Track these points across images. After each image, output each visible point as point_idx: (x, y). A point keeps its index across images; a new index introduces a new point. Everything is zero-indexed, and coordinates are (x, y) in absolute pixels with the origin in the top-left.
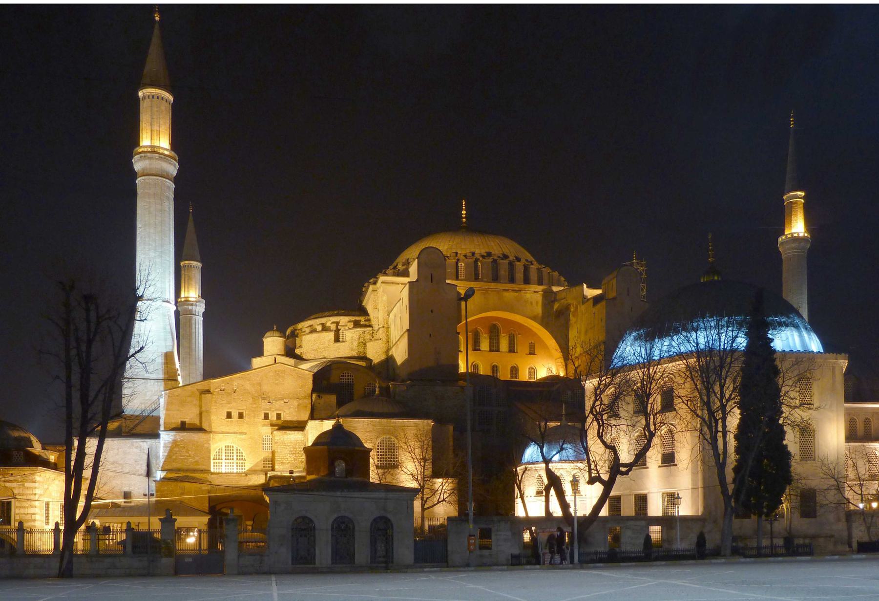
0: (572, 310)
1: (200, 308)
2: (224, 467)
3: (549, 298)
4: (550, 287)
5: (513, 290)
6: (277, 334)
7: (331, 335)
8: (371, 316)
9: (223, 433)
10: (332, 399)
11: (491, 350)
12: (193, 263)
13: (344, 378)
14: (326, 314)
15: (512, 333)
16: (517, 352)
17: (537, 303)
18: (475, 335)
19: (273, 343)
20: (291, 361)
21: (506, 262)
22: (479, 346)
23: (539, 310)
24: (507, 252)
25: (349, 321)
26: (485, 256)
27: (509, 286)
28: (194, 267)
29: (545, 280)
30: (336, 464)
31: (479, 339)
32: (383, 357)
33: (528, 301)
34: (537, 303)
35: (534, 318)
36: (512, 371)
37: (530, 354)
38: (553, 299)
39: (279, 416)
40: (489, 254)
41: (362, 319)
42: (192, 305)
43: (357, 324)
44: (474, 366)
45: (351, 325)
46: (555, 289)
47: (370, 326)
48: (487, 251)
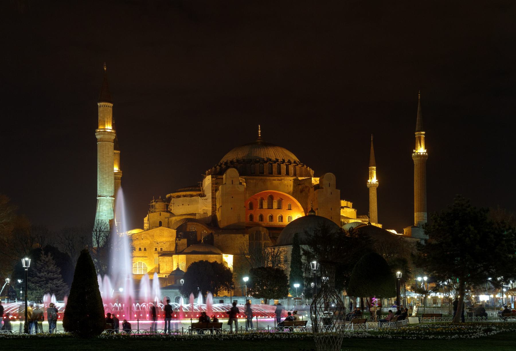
2: (138, 271)
4: (297, 177)
5: (278, 180)
9: (137, 257)
10: (185, 241)
16: (282, 209)
17: (291, 185)
20: (168, 215)
23: (291, 189)
29: (298, 172)
33: (286, 185)
34: (291, 185)
35: (289, 193)
36: (279, 218)
37: (289, 209)
38: (299, 183)
39: (161, 249)
46: (300, 178)
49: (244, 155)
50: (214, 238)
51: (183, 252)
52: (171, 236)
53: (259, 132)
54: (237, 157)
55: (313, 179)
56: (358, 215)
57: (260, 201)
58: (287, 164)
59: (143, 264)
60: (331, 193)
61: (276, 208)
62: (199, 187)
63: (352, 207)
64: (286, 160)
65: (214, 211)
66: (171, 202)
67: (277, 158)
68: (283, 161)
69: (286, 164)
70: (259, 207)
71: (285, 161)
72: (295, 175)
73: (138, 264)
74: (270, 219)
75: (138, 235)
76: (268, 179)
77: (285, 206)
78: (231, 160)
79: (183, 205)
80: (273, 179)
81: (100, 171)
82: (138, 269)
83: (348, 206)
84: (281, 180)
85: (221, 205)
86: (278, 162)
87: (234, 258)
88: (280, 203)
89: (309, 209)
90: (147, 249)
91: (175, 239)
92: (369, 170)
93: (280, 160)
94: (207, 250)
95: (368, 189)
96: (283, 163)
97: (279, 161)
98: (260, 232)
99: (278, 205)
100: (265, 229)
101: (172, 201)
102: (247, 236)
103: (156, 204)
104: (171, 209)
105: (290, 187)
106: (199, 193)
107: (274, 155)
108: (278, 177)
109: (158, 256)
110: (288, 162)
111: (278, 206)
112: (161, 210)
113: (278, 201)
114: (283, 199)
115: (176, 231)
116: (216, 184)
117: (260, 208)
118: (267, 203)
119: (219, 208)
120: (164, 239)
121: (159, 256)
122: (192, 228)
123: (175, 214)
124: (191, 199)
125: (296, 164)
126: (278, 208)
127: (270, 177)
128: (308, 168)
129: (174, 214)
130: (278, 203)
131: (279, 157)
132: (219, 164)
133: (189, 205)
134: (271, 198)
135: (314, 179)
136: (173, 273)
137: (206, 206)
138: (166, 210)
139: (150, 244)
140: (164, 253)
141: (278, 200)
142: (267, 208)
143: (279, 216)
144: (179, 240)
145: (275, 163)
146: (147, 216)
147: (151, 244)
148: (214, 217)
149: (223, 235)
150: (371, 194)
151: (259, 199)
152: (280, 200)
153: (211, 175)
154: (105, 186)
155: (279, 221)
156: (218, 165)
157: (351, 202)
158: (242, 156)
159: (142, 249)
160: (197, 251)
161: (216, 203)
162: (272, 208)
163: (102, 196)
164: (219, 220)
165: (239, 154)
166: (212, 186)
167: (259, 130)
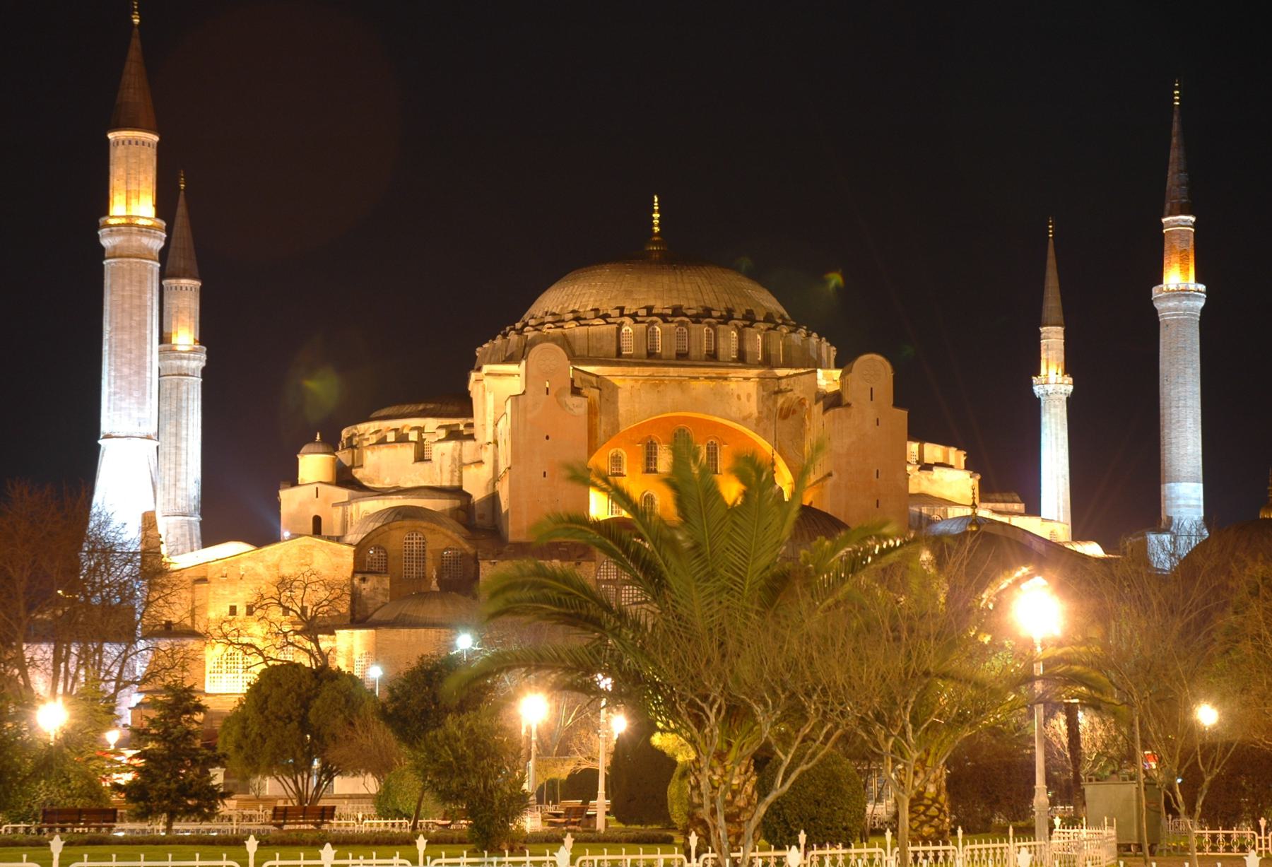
0: (808, 406)
1: (198, 362)
5: (706, 378)
6: (321, 448)
7: (408, 452)
8: (477, 420)
12: (184, 282)
13: (411, 541)
14: (407, 409)
15: (712, 442)
17: (749, 396)
18: (648, 448)
19: (313, 465)
20: (343, 494)
22: (655, 464)
23: (752, 407)
24: (709, 300)
25: (440, 427)
26: (668, 315)
28: (187, 289)
31: (656, 454)
32: (490, 492)
34: (749, 396)
35: (744, 420)
38: (776, 389)
40: (677, 311)
41: (460, 423)
42: (181, 358)
43: (453, 435)
44: (645, 500)
45: (442, 434)
46: (781, 372)
47: (471, 437)
48: (676, 302)
53: (653, 219)
55: (819, 370)
56: (987, 491)
58: (740, 324)
63: (963, 465)
64: (738, 311)
69: (736, 325)
71: (735, 317)
75: (226, 564)
81: (110, 354)
83: (948, 460)
85: (508, 466)
86: (710, 316)
92: (1042, 336)
95: (1040, 398)
96: (726, 323)
97: (714, 314)
105: (748, 400)
108: (708, 370)
110: (745, 318)
125: (772, 325)
127: (682, 369)
135: (824, 375)
144: (364, 580)
150: (1045, 419)
154: (127, 401)
156: (514, 329)
157: (959, 449)
159: (238, 610)
163: (116, 434)
164: (504, 510)
167: (653, 211)
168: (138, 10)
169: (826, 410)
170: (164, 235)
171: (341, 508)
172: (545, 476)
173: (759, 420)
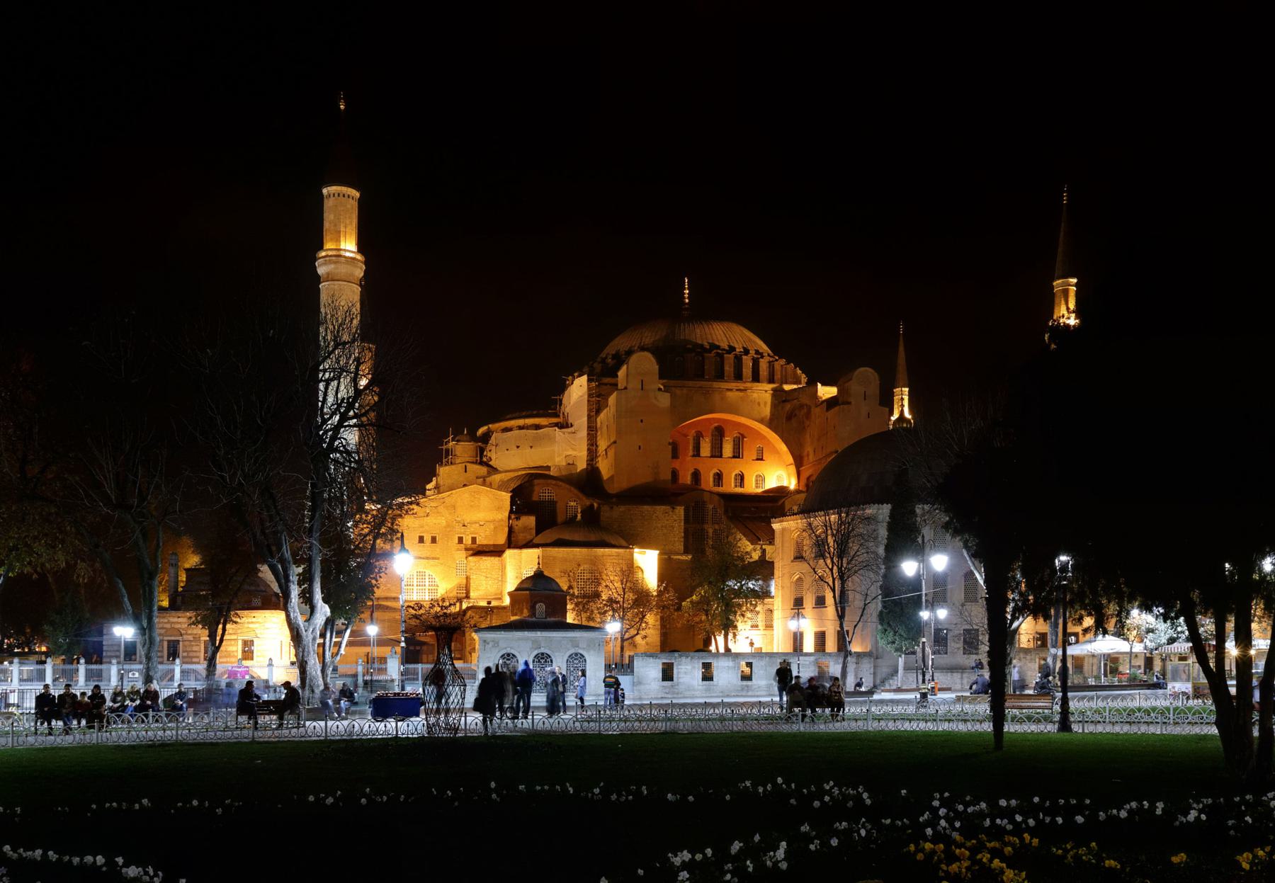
2: (415, 594)
3: (780, 397)
5: (737, 390)
10: (530, 521)
11: (712, 457)
16: (742, 458)
21: (731, 356)
23: (767, 411)
27: (733, 385)
29: (778, 376)
30: (537, 607)
34: (766, 403)
35: (761, 421)
37: (758, 459)
38: (784, 399)
39: (474, 540)
46: (787, 387)
49: (657, 338)
50: (602, 513)
51: (531, 544)
52: (499, 508)
53: (684, 294)
54: (641, 343)
55: (819, 385)
57: (694, 439)
58: (755, 356)
59: (427, 577)
60: (869, 414)
61: (731, 456)
62: (555, 409)
65: (592, 460)
66: (490, 442)
67: (732, 344)
68: (746, 352)
70: (691, 453)
72: (771, 381)
73: (415, 574)
74: (714, 481)
76: (717, 387)
77: (749, 452)
78: (627, 350)
79: (518, 447)
80: (727, 387)
82: (415, 588)
84: (746, 390)
87: (660, 554)
88: (739, 442)
89: (808, 456)
90: (437, 539)
91: (507, 514)
93: (739, 349)
94: (593, 537)
97: (738, 350)
98: (704, 502)
99: (734, 448)
100: (717, 498)
101: (493, 440)
102: (680, 511)
103: (457, 446)
104: (490, 458)
105: (765, 406)
106: (555, 420)
107: (725, 339)
109: (465, 556)
111: (734, 452)
112: (467, 459)
113: (734, 441)
114: (746, 434)
115: (510, 494)
116: (598, 396)
117: (694, 456)
118: (710, 445)
119: (608, 447)
120: (480, 516)
121: (466, 558)
122: (542, 493)
123: (499, 469)
124: (537, 433)
126: (734, 457)
128: (798, 368)
129: (496, 469)
130: (734, 445)
131: (735, 341)
132: (599, 360)
133: (531, 447)
134: (719, 433)
136: (525, 586)
137: (572, 449)
138: (478, 458)
139: (445, 527)
140: (479, 549)
141: (734, 438)
142: (709, 455)
143: (736, 475)
144: (518, 519)
145: (730, 353)
146: (432, 481)
147: (448, 526)
148: (592, 472)
149: (622, 508)
151: (693, 433)
152: (739, 438)
153: (588, 376)
155: (736, 486)
158: (652, 340)
159: (425, 539)
160: (568, 540)
161: (596, 440)
162: (721, 456)
165: (646, 335)
166: (588, 401)
167: (685, 289)
168: (343, 99)
169: (828, 410)
170: (364, 267)
171: (482, 479)
172: (640, 448)
173: (771, 420)
